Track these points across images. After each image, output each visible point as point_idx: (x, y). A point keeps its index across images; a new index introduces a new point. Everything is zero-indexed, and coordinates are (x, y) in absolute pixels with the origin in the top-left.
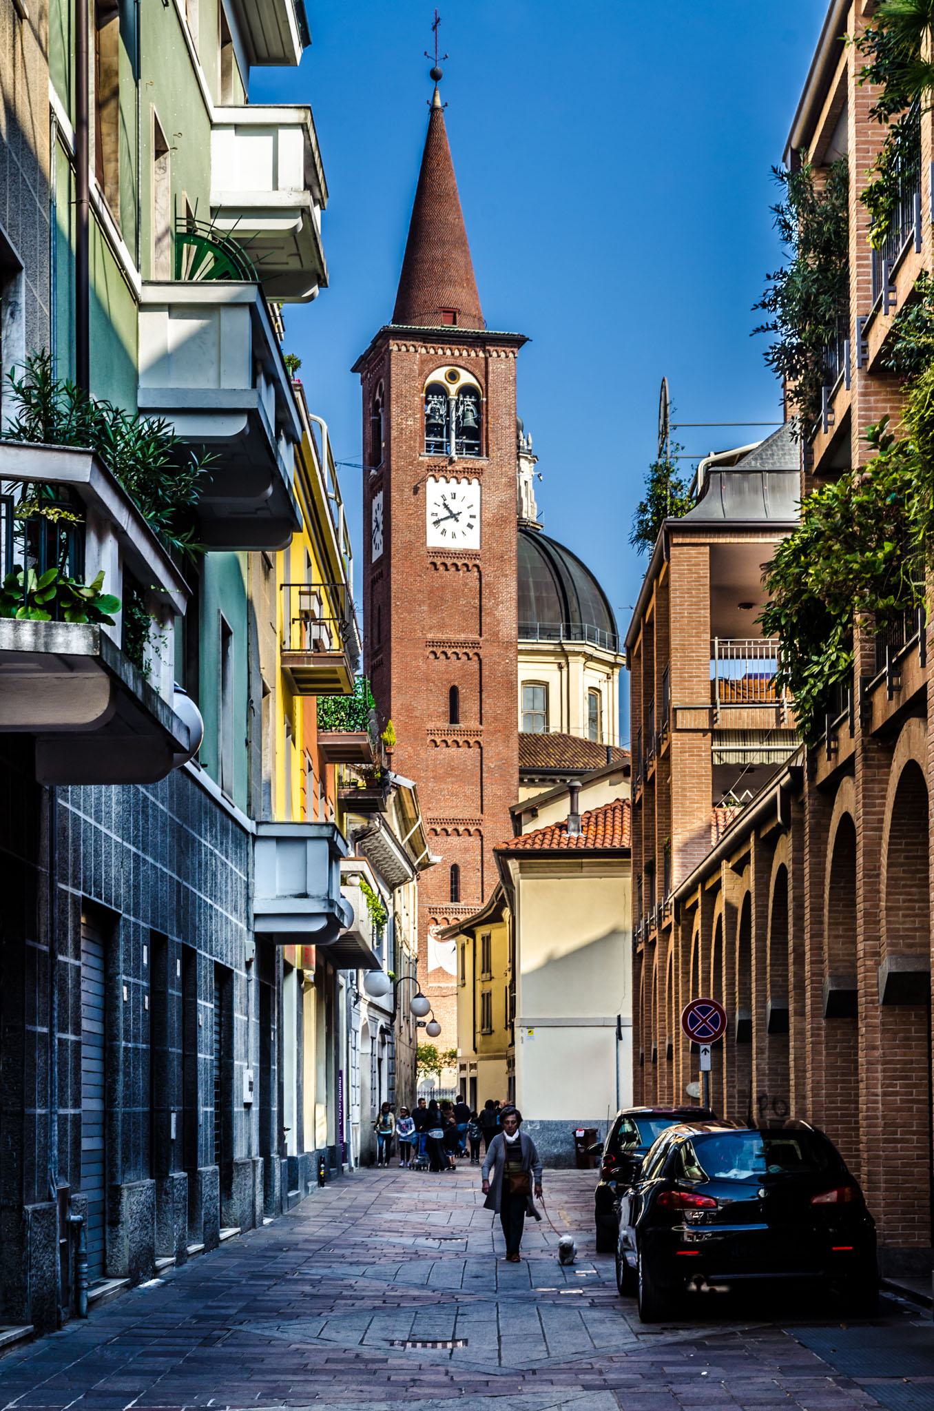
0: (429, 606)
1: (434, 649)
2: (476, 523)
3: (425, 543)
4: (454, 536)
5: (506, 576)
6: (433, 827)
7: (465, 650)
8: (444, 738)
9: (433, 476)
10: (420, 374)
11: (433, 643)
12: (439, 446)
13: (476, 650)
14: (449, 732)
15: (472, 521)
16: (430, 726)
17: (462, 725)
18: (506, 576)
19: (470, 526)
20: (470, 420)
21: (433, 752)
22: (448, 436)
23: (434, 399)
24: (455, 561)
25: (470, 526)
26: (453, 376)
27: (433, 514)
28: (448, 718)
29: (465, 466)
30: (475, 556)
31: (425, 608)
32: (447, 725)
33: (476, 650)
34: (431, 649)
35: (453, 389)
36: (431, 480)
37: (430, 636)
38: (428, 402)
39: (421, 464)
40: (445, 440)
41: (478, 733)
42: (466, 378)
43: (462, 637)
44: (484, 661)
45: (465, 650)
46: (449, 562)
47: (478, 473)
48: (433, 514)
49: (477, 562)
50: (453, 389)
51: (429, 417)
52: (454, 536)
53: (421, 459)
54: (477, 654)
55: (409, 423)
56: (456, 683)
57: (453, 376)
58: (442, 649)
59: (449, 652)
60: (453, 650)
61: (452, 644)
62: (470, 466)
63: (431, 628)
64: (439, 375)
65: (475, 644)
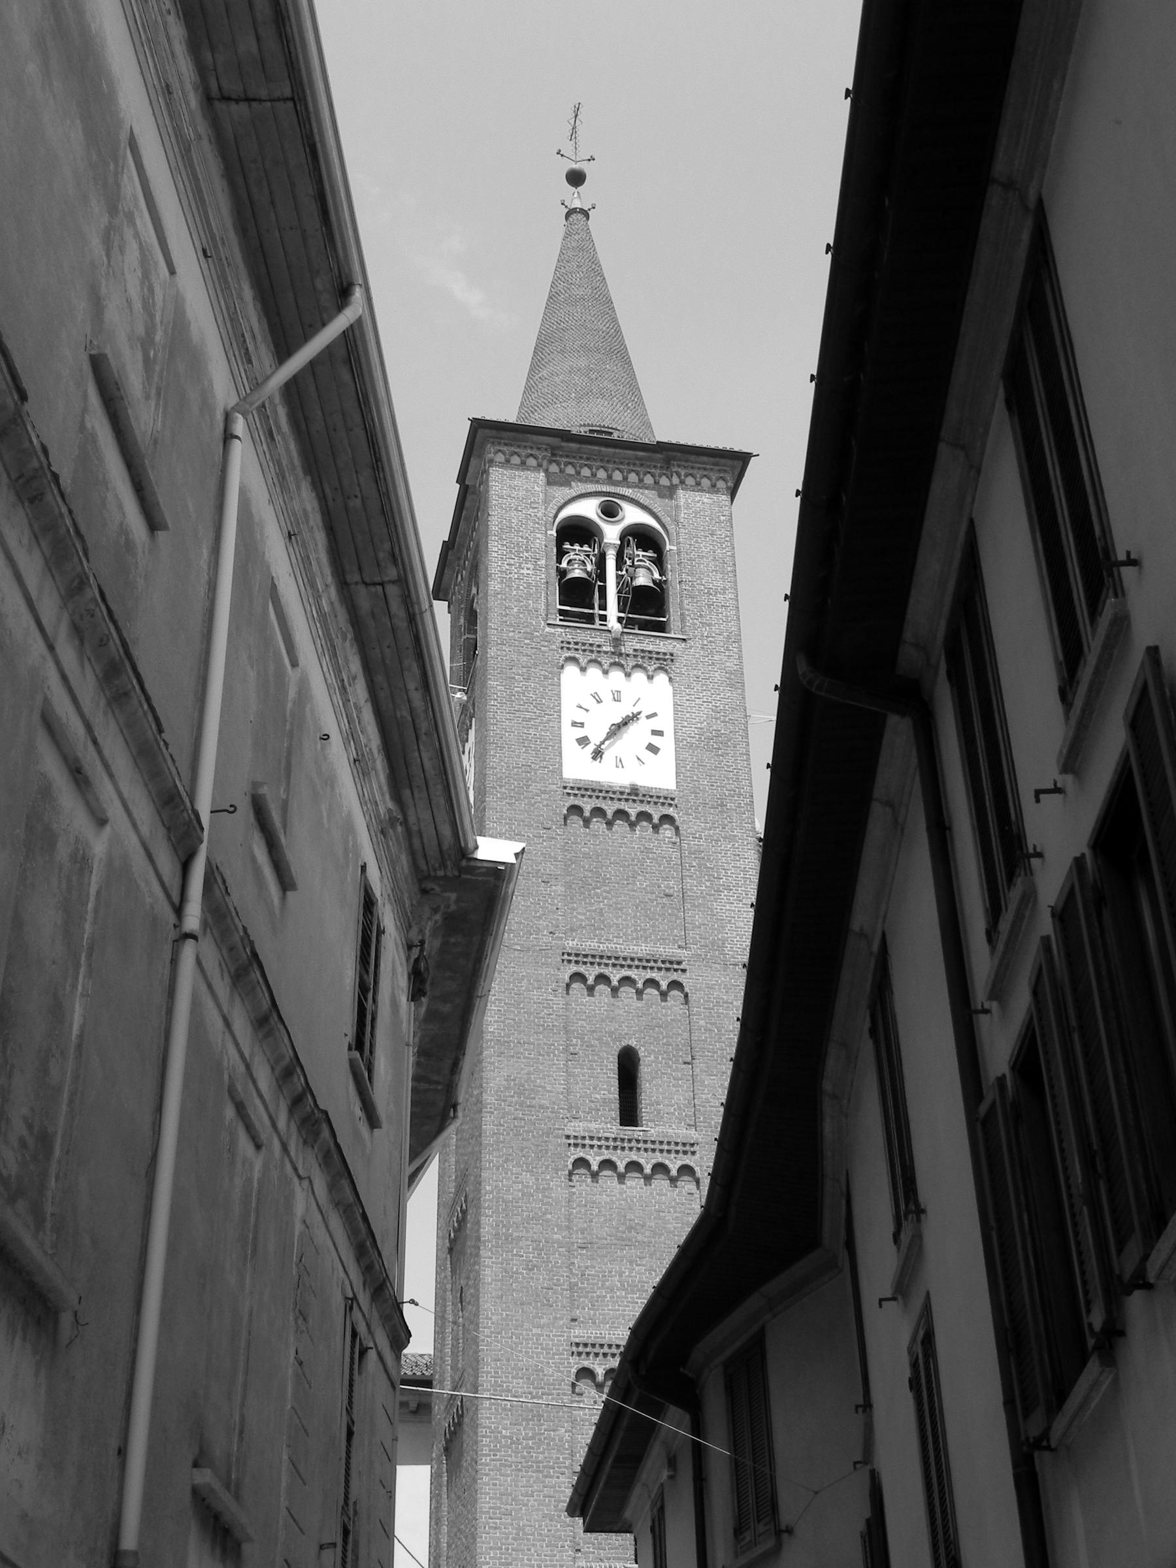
0: (568, 886)
1: (581, 969)
2: (667, 744)
3: (559, 770)
4: (620, 763)
5: (732, 839)
6: (586, 1363)
7: (650, 974)
8: (607, 1155)
9: (573, 659)
10: (546, 502)
11: (579, 957)
12: (590, 619)
13: (675, 976)
14: (618, 1144)
15: (656, 741)
16: (576, 1128)
17: (650, 1128)
18: (732, 839)
19: (653, 749)
20: (642, 580)
21: (583, 1184)
22: (603, 607)
23: (576, 551)
24: (624, 806)
25: (653, 749)
26: (610, 511)
27: (574, 724)
28: (615, 1114)
29: (638, 647)
30: (666, 799)
31: (560, 889)
32: (614, 1128)
33: (675, 976)
34: (574, 968)
35: (611, 533)
36: (571, 671)
37: (571, 944)
38: (561, 554)
39: (547, 639)
40: (597, 611)
41: (688, 1148)
42: (632, 515)
43: (642, 949)
44: (692, 997)
45: (650, 974)
46: (610, 808)
47: (663, 663)
48: (574, 724)
49: (670, 811)
50: (611, 533)
51: (562, 573)
52: (620, 763)
53: (548, 629)
54: (676, 985)
55: (525, 572)
56: (633, 1043)
57: (610, 511)
58: (597, 970)
59: (615, 976)
60: (625, 972)
61: (618, 961)
62: (650, 648)
63: (572, 930)
64: (588, 509)
65: (672, 964)
